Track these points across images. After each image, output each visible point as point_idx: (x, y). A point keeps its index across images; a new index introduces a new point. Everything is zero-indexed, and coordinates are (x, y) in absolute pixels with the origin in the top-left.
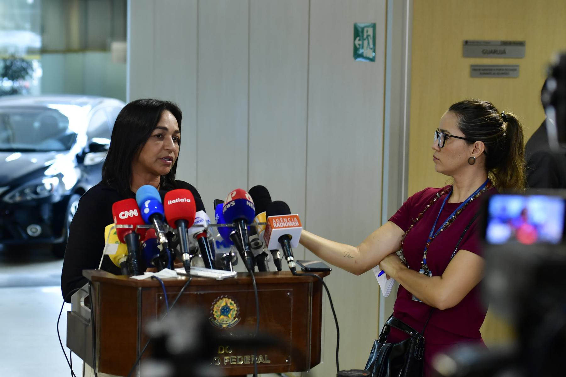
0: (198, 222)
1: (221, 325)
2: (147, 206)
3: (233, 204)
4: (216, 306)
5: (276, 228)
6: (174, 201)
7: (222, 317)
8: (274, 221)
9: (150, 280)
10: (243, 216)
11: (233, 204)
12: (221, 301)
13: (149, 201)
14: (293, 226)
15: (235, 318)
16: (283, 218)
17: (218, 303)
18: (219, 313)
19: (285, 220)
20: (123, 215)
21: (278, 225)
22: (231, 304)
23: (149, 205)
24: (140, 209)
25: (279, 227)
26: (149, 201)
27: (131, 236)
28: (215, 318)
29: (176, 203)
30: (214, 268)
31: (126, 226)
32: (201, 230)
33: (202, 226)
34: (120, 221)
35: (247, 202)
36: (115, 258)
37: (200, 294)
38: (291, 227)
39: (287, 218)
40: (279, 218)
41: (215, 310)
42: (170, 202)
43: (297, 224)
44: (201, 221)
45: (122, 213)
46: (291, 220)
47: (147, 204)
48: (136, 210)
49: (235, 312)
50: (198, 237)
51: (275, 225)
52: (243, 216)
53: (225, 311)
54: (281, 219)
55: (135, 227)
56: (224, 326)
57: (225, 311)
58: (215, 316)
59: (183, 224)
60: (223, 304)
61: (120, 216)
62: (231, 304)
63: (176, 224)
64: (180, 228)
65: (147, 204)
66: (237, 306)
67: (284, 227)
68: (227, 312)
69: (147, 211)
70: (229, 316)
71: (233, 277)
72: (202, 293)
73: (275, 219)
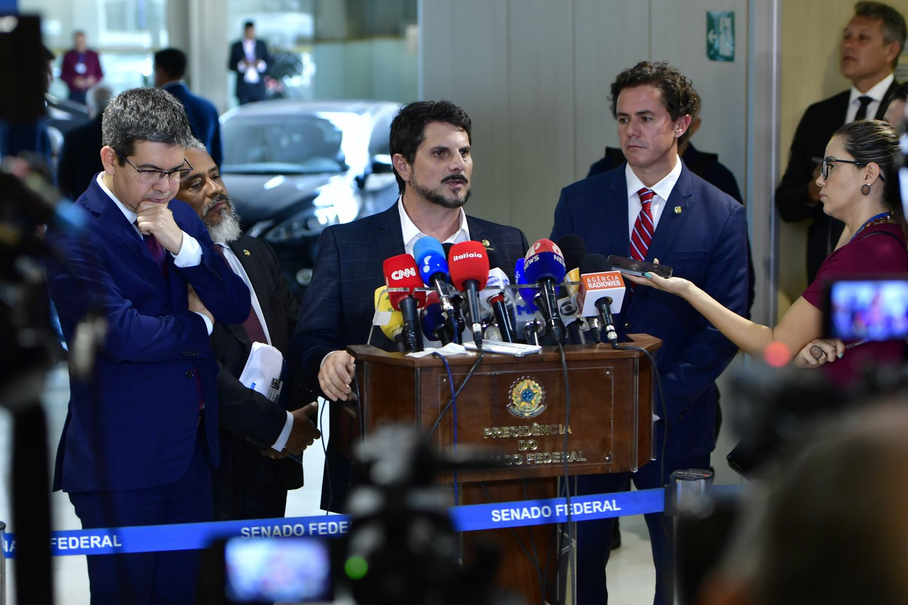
1: (522, 413)
2: (427, 263)
3: (537, 258)
4: (515, 389)
6: (461, 257)
7: (523, 403)
9: (431, 358)
10: (549, 275)
11: (537, 258)
12: (521, 383)
13: (430, 257)
14: (614, 287)
15: (540, 405)
16: (600, 275)
17: (518, 386)
18: (519, 399)
19: (603, 278)
20: (397, 275)
21: (594, 285)
22: (534, 386)
23: (430, 261)
24: (419, 266)
25: (595, 288)
26: (430, 257)
27: (408, 303)
30: (513, 342)
31: (401, 290)
32: (496, 293)
33: (497, 287)
34: (393, 283)
36: (388, 329)
39: (605, 275)
40: (595, 276)
41: (514, 395)
42: (456, 258)
45: (396, 273)
46: (610, 278)
47: (427, 260)
48: (412, 269)
49: (540, 397)
50: (492, 301)
51: (590, 286)
52: (549, 275)
53: (527, 396)
55: (412, 290)
56: (527, 415)
57: (527, 396)
59: (473, 286)
60: (525, 387)
61: (393, 276)
62: (534, 386)
63: (464, 286)
64: (469, 291)
65: (427, 260)
66: (543, 390)
68: (530, 397)
69: (426, 269)
70: (533, 402)
71: (536, 353)
72: (497, 373)
73: (590, 277)
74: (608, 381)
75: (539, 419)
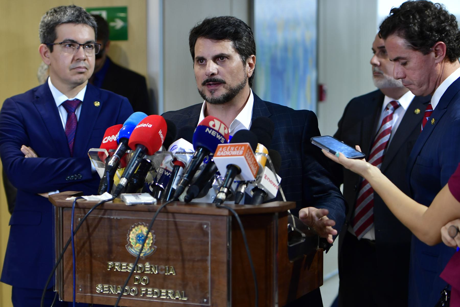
4: (131, 232)
5: (218, 156)
8: (221, 149)
14: (236, 155)
15: (150, 247)
16: (231, 146)
17: (134, 230)
18: (135, 241)
19: (232, 148)
20: (106, 140)
21: (222, 154)
25: (221, 156)
28: (131, 246)
35: (208, 129)
37: (117, 219)
38: (234, 155)
41: (130, 236)
43: (241, 152)
44: (176, 148)
49: (151, 242)
51: (218, 153)
52: (200, 144)
54: (229, 147)
58: (132, 244)
59: (140, 149)
67: (226, 156)
72: (119, 218)
74: (205, 234)
75: (148, 258)
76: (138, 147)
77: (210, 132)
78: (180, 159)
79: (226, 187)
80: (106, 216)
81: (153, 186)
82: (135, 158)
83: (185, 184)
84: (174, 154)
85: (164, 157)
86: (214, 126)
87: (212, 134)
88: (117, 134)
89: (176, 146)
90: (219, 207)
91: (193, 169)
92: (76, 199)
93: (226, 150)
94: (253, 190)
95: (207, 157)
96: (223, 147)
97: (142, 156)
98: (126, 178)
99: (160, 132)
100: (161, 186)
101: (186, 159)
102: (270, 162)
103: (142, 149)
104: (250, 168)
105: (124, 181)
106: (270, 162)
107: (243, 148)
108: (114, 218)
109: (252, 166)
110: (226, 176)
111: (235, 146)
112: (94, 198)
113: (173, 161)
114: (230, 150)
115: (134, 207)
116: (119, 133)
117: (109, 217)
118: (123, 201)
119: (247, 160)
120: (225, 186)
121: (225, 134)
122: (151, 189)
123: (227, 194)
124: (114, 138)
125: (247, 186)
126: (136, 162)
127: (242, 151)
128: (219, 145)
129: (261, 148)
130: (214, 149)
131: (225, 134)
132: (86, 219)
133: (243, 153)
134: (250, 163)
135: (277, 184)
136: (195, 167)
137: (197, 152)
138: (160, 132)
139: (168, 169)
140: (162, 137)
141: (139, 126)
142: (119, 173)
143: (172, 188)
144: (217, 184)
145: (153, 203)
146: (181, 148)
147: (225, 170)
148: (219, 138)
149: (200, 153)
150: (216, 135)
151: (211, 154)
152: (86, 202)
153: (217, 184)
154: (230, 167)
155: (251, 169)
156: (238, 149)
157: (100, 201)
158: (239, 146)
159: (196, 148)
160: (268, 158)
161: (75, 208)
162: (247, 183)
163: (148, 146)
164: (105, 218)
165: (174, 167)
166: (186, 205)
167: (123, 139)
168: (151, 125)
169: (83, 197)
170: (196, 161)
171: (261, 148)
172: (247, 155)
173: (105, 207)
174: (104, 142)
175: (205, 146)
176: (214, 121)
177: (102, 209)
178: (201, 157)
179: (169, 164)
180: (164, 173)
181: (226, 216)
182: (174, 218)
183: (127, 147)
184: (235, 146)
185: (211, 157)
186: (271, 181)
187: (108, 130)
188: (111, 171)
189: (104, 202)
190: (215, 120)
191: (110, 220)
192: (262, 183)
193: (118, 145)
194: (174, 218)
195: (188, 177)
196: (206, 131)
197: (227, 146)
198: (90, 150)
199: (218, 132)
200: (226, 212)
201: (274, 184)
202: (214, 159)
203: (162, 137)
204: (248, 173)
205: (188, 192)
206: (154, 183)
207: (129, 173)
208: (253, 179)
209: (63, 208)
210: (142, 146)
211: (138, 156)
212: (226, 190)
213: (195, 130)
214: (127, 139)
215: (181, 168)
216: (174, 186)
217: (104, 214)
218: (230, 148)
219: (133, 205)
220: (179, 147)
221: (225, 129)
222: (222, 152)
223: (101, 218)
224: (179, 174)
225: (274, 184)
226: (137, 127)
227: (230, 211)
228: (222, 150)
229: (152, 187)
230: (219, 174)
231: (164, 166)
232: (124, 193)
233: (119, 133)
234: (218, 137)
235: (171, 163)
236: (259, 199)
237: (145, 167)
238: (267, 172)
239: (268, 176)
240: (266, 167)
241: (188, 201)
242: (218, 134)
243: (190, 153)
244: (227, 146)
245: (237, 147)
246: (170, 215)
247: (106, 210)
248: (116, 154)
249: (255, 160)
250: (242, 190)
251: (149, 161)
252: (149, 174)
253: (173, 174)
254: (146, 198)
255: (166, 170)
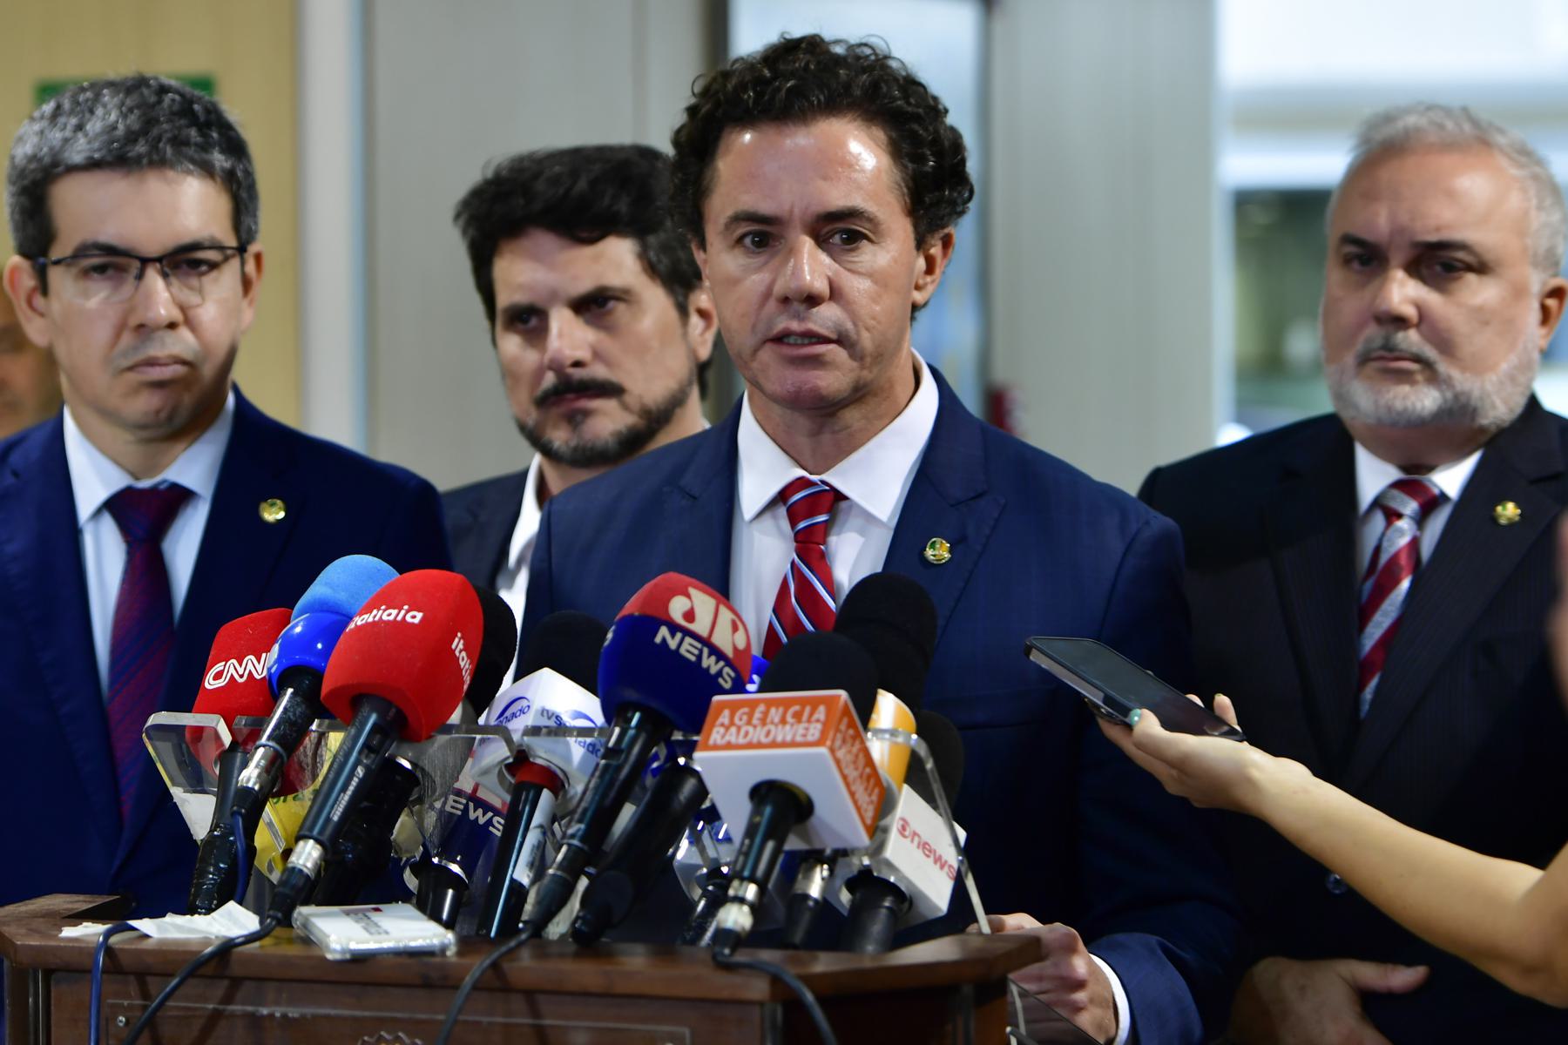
0: (514, 715)
5: (716, 747)
8: (725, 717)
14: (794, 744)
16: (770, 704)
20: (218, 676)
21: (732, 736)
25: (729, 746)
29: (367, 624)
35: (664, 631)
37: (284, 1016)
38: (784, 745)
43: (815, 731)
44: (522, 711)
51: (716, 735)
52: (631, 694)
54: (761, 708)
59: (373, 718)
67: (750, 746)
72: (294, 1013)
76: (365, 710)
77: (673, 644)
78: (544, 752)
79: (752, 879)
80: (235, 1008)
81: (422, 867)
82: (355, 754)
83: (573, 868)
84: (516, 737)
85: (468, 750)
86: (690, 615)
87: (683, 651)
88: (268, 650)
89: (524, 703)
90: (729, 967)
91: (608, 802)
92: (108, 934)
93: (749, 722)
94: (851, 885)
95: (661, 750)
96: (734, 707)
97: (382, 743)
98: (317, 841)
99: (458, 644)
100: (455, 868)
101: (568, 758)
102: (929, 765)
103: (381, 716)
104: (852, 794)
105: (308, 855)
106: (929, 765)
107: (821, 713)
108: (271, 1016)
109: (859, 788)
110: (751, 831)
111: (787, 704)
112: (179, 928)
113: (509, 767)
114: (763, 722)
115: (362, 969)
116: (276, 648)
117: (250, 1008)
118: (307, 941)
119: (838, 762)
120: (746, 873)
121: (735, 649)
122: (411, 881)
123: (755, 909)
124: (259, 666)
125: (831, 870)
126: (360, 771)
127: (819, 726)
128: (716, 698)
129: (888, 708)
130: (697, 720)
131: (735, 649)
132: (151, 1023)
133: (824, 733)
134: (852, 774)
135: (953, 858)
136: (612, 794)
137: (617, 730)
138: (458, 644)
139: (481, 794)
140: (465, 663)
141: (368, 618)
142: (277, 816)
143: (513, 880)
144: (696, 859)
145: (443, 949)
146: (544, 712)
147: (746, 807)
148: (713, 670)
149: (631, 732)
150: (699, 657)
151: (678, 736)
152: (146, 944)
153: (696, 859)
154: (765, 792)
155: (855, 802)
156: (798, 716)
157: (206, 941)
158: (803, 702)
159: (612, 711)
160: (923, 750)
161: (104, 971)
162: (835, 858)
163: (406, 701)
164: (233, 1015)
165: (516, 791)
166: (578, 955)
167: (297, 673)
168: (419, 615)
169: (133, 923)
170: (619, 768)
171: (888, 708)
172: (838, 743)
173: (236, 970)
174: (210, 683)
175: (655, 705)
176: (688, 596)
177: (222, 977)
178: (636, 749)
179: (493, 778)
180: (466, 810)
181: (761, 1004)
182: (535, 1012)
183: (315, 705)
184: (787, 704)
185: (689, 748)
186: (925, 847)
187: (226, 633)
188: (243, 810)
189: (227, 948)
190: (692, 591)
191: (255, 1021)
192: (889, 853)
193: (276, 698)
194: (535, 1012)
195: (584, 838)
196: (658, 640)
197: (753, 705)
198: (153, 720)
199: (706, 642)
200: (758, 989)
201: (938, 860)
202: (701, 760)
203: (465, 663)
204: (838, 815)
205: (584, 902)
206: (426, 856)
207: (328, 819)
208: (864, 840)
209: (49, 973)
210: (382, 703)
211: (366, 745)
212: (751, 891)
213: (610, 636)
214: (317, 675)
215: (546, 795)
216: (521, 872)
217: (228, 999)
218: (766, 714)
219: (360, 959)
220: (537, 705)
221: (735, 629)
222: (733, 730)
223: (216, 1016)
224: (538, 818)
225: (938, 860)
226: (359, 621)
227: (776, 980)
228: (732, 723)
229: (415, 873)
230: (713, 816)
231: (465, 783)
232: (306, 903)
233: (276, 648)
234: (709, 662)
235: (500, 773)
236: (878, 926)
237: (387, 790)
238: (910, 804)
239: (914, 825)
240: (906, 787)
241: (586, 939)
242: (706, 651)
243: (583, 732)
244: (753, 705)
245: (797, 708)
246: (518, 1003)
247: (236, 982)
248: (269, 738)
249: (869, 761)
250: (815, 889)
251: (407, 765)
252: (403, 818)
253: (515, 819)
254: (405, 929)
255: (475, 799)
